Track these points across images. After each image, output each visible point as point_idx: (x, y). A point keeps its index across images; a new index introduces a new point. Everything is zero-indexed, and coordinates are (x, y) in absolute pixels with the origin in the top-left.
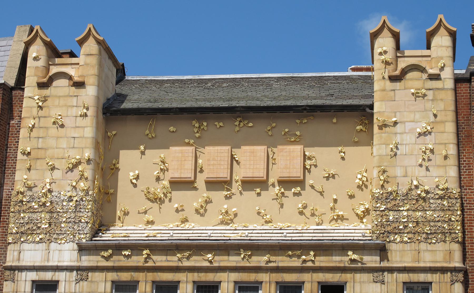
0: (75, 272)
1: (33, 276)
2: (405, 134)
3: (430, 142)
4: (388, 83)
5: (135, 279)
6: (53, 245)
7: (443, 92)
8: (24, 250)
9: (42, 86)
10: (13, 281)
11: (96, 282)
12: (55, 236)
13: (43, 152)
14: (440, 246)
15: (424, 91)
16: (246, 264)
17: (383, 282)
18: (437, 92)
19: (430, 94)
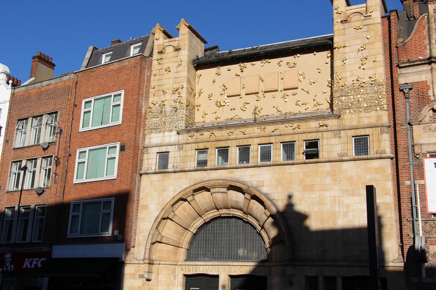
0: (177, 146)
1: (157, 150)
2: (351, 53)
3: (365, 53)
5: (207, 147)
7: (374, 25)
8: (152, 138)
10: (148, 153)
11: (187, 150)
13: (161, 86)
14: (373, 113)
15: (361, 27)
16: (263, 133)
17: (340, 137)
18: (370, 26)
19: (365, 28)
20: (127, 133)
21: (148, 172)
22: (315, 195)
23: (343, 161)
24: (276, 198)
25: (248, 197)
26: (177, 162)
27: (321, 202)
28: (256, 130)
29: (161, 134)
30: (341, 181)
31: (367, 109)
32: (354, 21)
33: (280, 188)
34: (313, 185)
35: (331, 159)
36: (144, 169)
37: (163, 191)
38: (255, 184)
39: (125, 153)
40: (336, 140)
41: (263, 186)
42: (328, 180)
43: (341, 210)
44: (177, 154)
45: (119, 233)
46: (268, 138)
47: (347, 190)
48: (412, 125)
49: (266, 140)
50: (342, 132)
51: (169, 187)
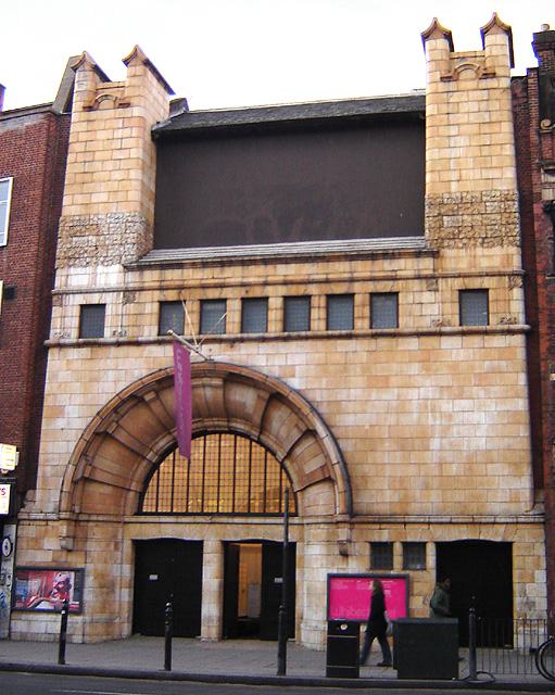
6: (100, 268)
9: (89, 109)
10: (61, 305)
12: (102, 259)
14: (497, 250)
17: (437, 290)
21: (62, 341)
22: (390, 395)
23: (441, 334)
24: (319, 399)
27: (402, 410)
29: (89, 270)
31: (485, 241)
33: (324, 381)
34: (387, 377)
35: (420, 330)
38: (276, 372)
40: (427, 297)
41: (294, 376)
42: (415, 368)
43: (438, 422)
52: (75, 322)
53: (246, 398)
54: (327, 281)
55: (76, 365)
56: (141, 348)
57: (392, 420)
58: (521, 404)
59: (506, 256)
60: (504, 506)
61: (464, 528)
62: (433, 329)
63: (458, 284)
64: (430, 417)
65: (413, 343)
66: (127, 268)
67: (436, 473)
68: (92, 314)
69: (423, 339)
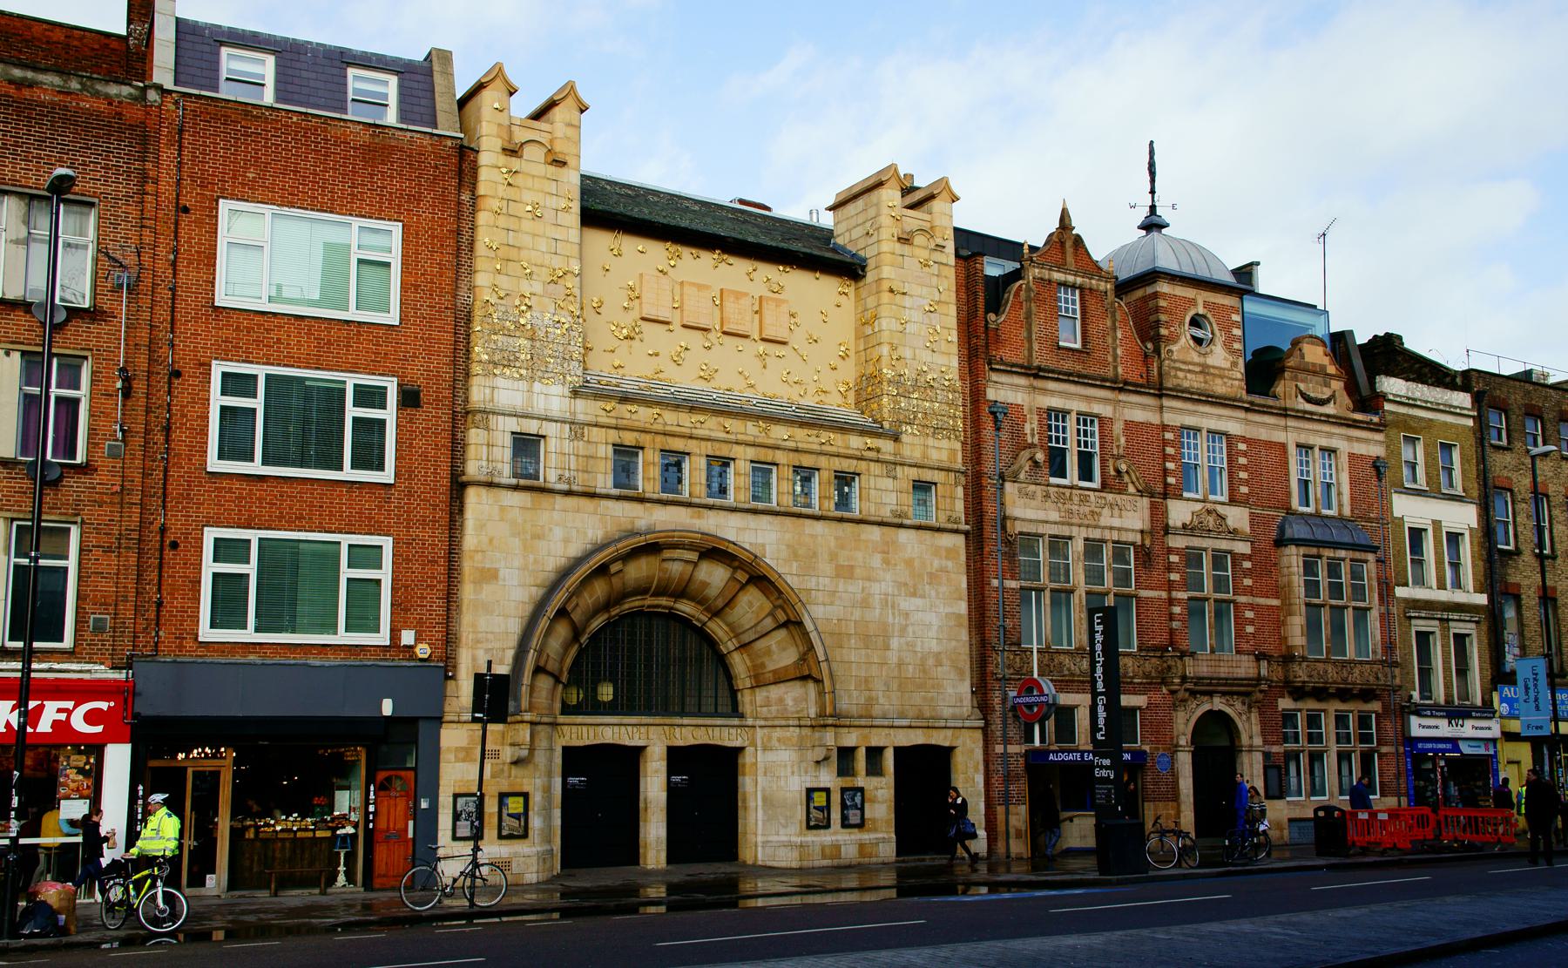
4: (898, 245)
5: (641, 445)
6: (537, 386)
10: (487, 429)
12: (539, 373)
14: (945, 443)
17: (895, 478)
18: (942, 267)
20: (424, 358)
22: (855, 588)
23: (901, 526)
25: (742, 577)
26: (569, 469)
27: (865, 604)
28: (751, 430)
30: (896, 565)
32: (919, 246)
34: (852, 567)
36: (474, 468)
37: (537, 537)
39: (419, 414)
40: (888, 483)
42: (876, 561)
43: (896, 621)
44: (567, 446)
45: (418, 640)
46: (770, 452)
47: (906, 584)
48: (1004, 481)
49: (768, 455)
50: (899, 468)
51: (551, 529)
52: (508, 454)
53: (714, 576)
54: (796, 450)
55: (516, 514)
56: (596, 501)
57: (857, 614)
58: (962, 607)
59: (947, 450)
60: (951, 710)
61: (919, 731)
62: (889, 518)
63: (914, 473)
64: (890, 616)
65: (875, 533)
66: (575, 393)
67: (896, 673)
68: (525, 445)
69: (885, 529)
